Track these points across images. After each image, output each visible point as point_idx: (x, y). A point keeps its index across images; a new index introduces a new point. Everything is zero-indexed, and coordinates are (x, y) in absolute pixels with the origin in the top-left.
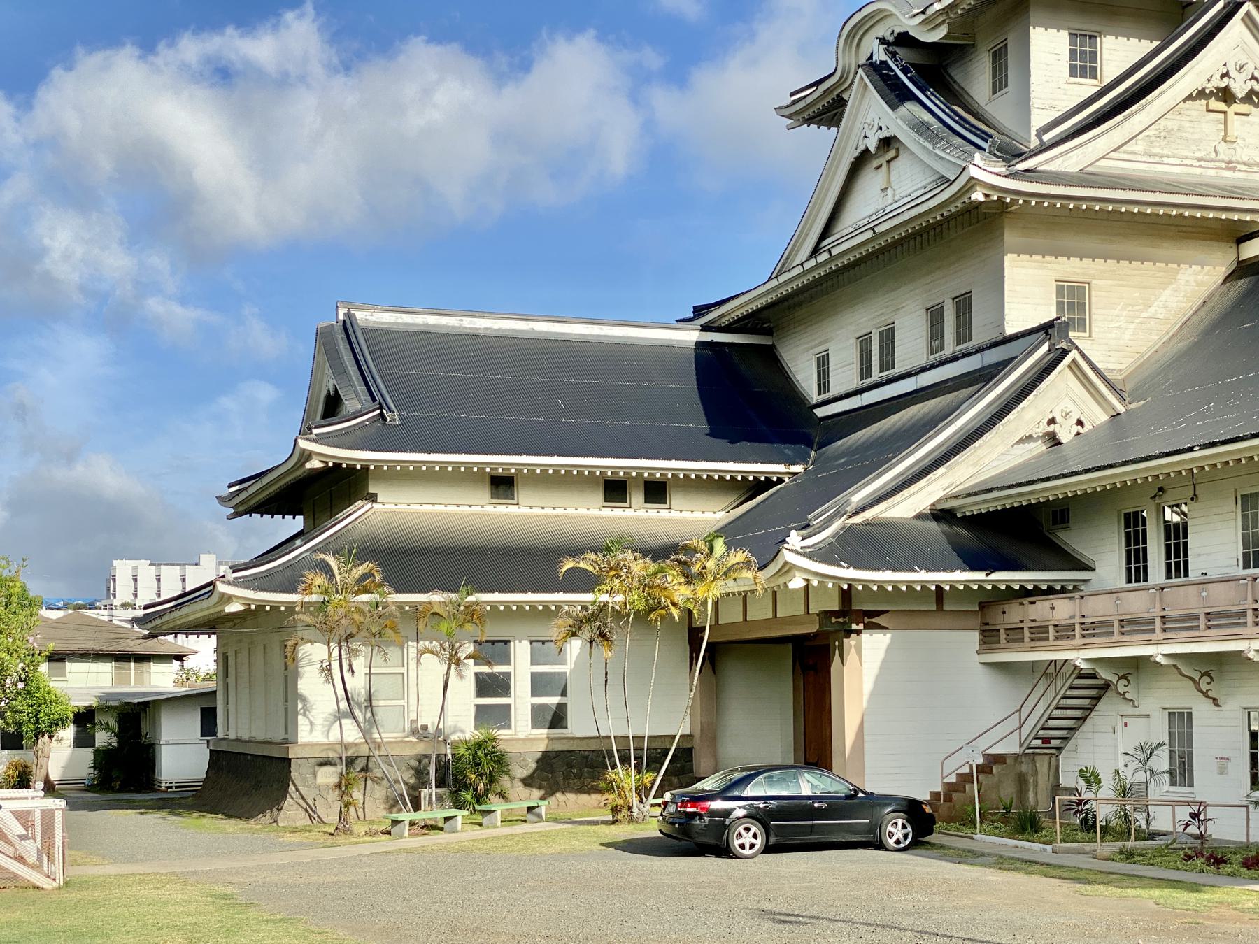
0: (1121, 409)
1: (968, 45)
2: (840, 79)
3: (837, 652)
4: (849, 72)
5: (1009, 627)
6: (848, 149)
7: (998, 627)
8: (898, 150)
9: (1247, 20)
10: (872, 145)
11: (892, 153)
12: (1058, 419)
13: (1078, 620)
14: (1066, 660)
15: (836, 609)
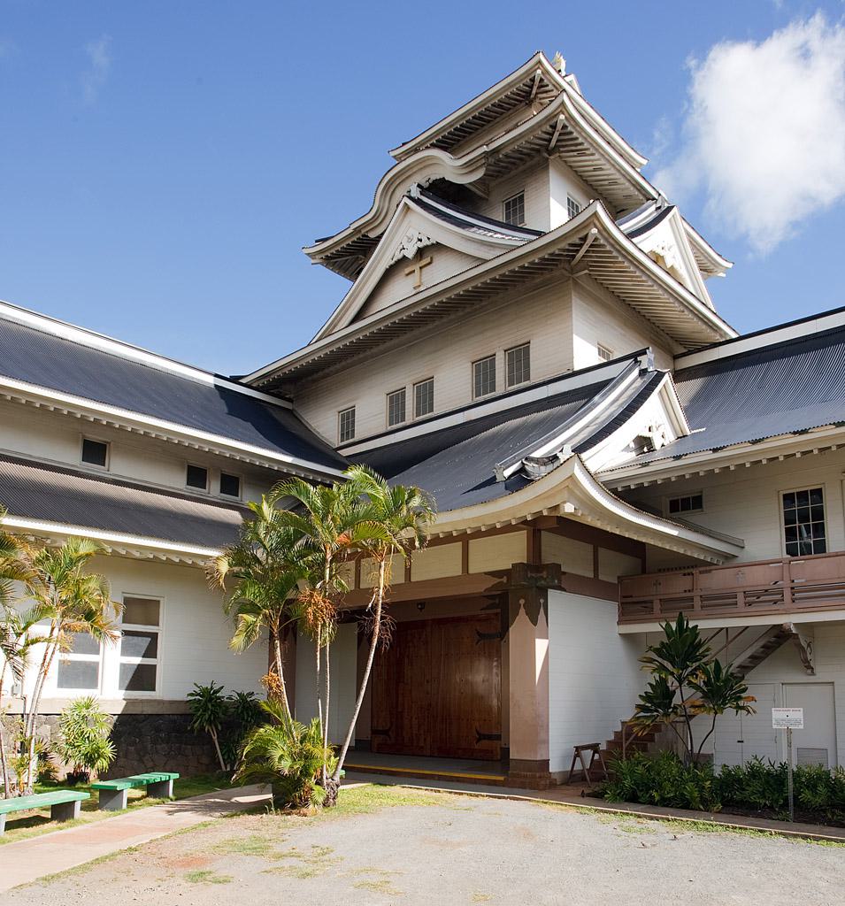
0: (689, 433)
1: (484, 199)
2: (375, 218)
3: (522, 611)
4: (382, 210)
5: (665, 597)
6: (385, 258)
7: (651, 598)
8: (432, 258)
9: (673, 219)
10: (410, 253)
11: (428, 260)
12: (654, 429)
13: (785, 584)
14: (748, 627)
15: (525, 562)
